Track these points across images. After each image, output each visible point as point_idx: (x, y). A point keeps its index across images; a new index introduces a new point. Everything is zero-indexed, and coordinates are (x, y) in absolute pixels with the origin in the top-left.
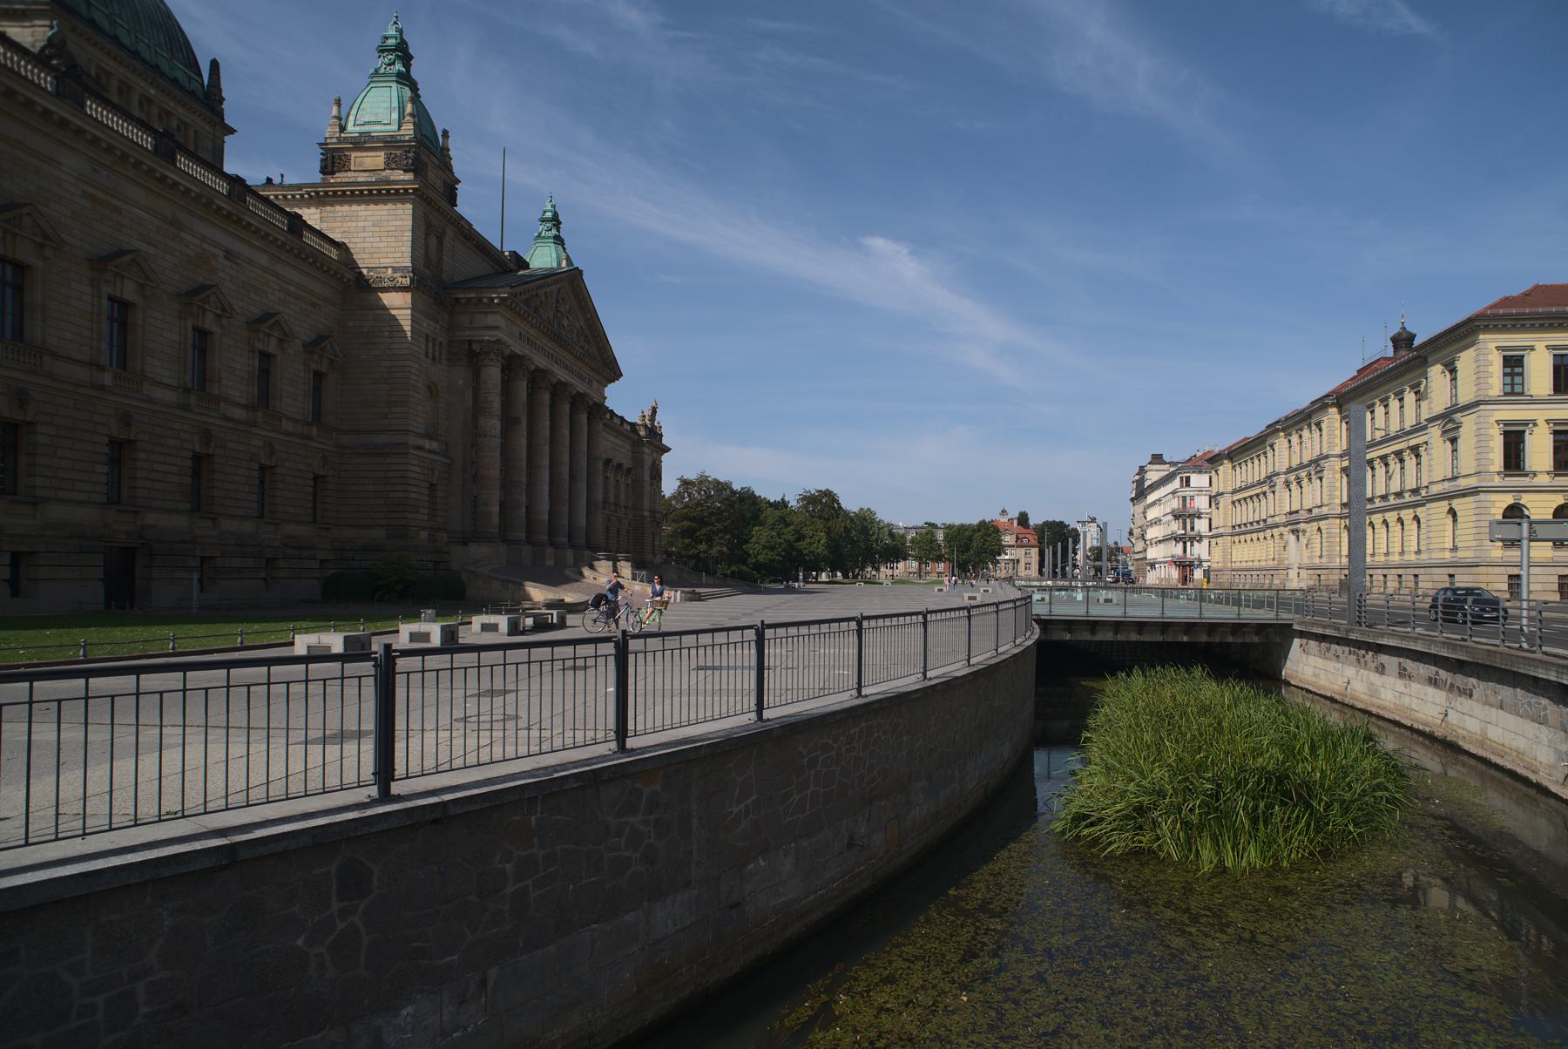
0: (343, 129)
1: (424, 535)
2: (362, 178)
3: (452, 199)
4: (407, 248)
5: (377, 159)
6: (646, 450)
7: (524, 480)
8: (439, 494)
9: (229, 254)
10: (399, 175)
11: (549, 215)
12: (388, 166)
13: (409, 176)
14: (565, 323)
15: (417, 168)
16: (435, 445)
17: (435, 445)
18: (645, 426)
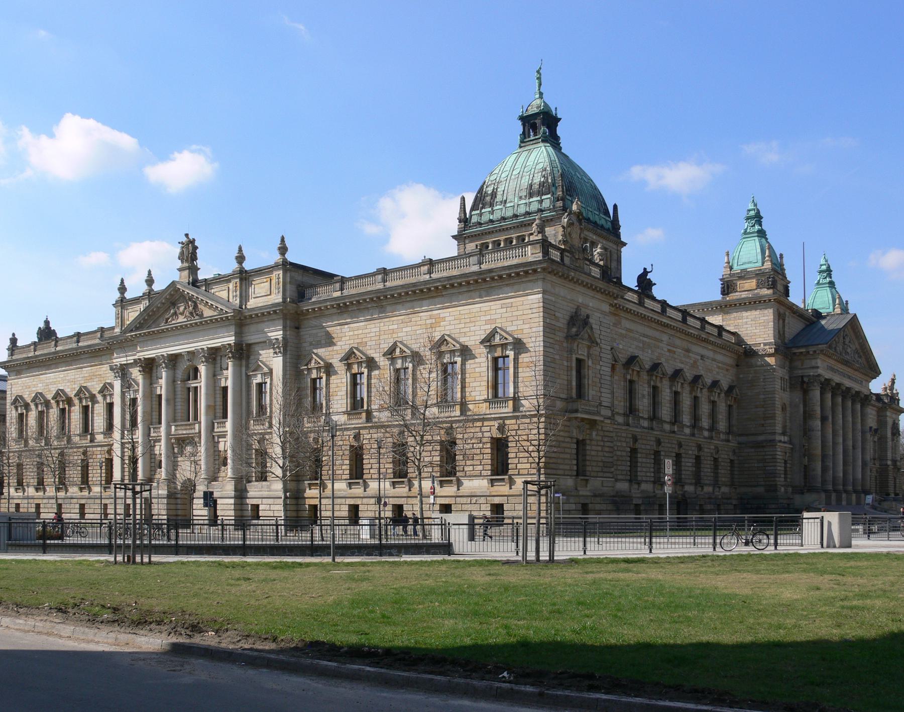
0: (731, 268)
2: (744, 295)
3: (787, 293)
4: (771, 332)
5: (752, 284)
6: (888, 414)
7: (831, 453)
9: (702, 357)
10: (766, 292)
11: (824, 267)
12: (758, 287)
13: (770, 292)
15: (773, 286)
16: (786, 439)
18: (887, 395)
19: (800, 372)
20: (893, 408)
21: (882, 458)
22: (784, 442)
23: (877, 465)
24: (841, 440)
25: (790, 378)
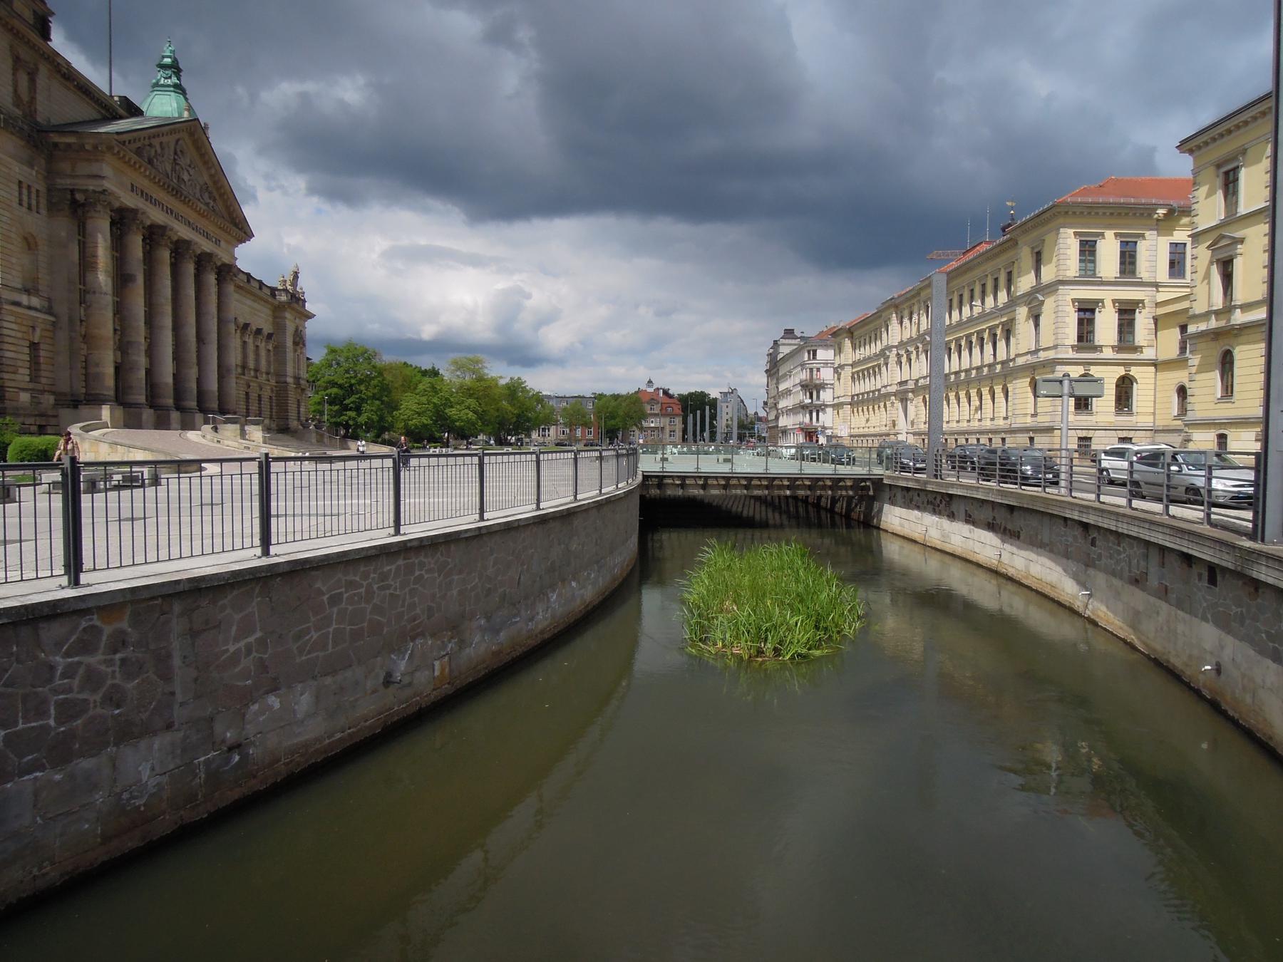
1: (25, 397)
6: (288, 315)
8: (42, 353)
14: (186, 177)
16: (35, 301)
17: (35, 301)
18: (286, 290)
19: (65, 182)
20: (293, 309)
21: (280, 375)
22: (30, 308)
23: (273, 382)
24: (167, 321)
25: (49, 190)
